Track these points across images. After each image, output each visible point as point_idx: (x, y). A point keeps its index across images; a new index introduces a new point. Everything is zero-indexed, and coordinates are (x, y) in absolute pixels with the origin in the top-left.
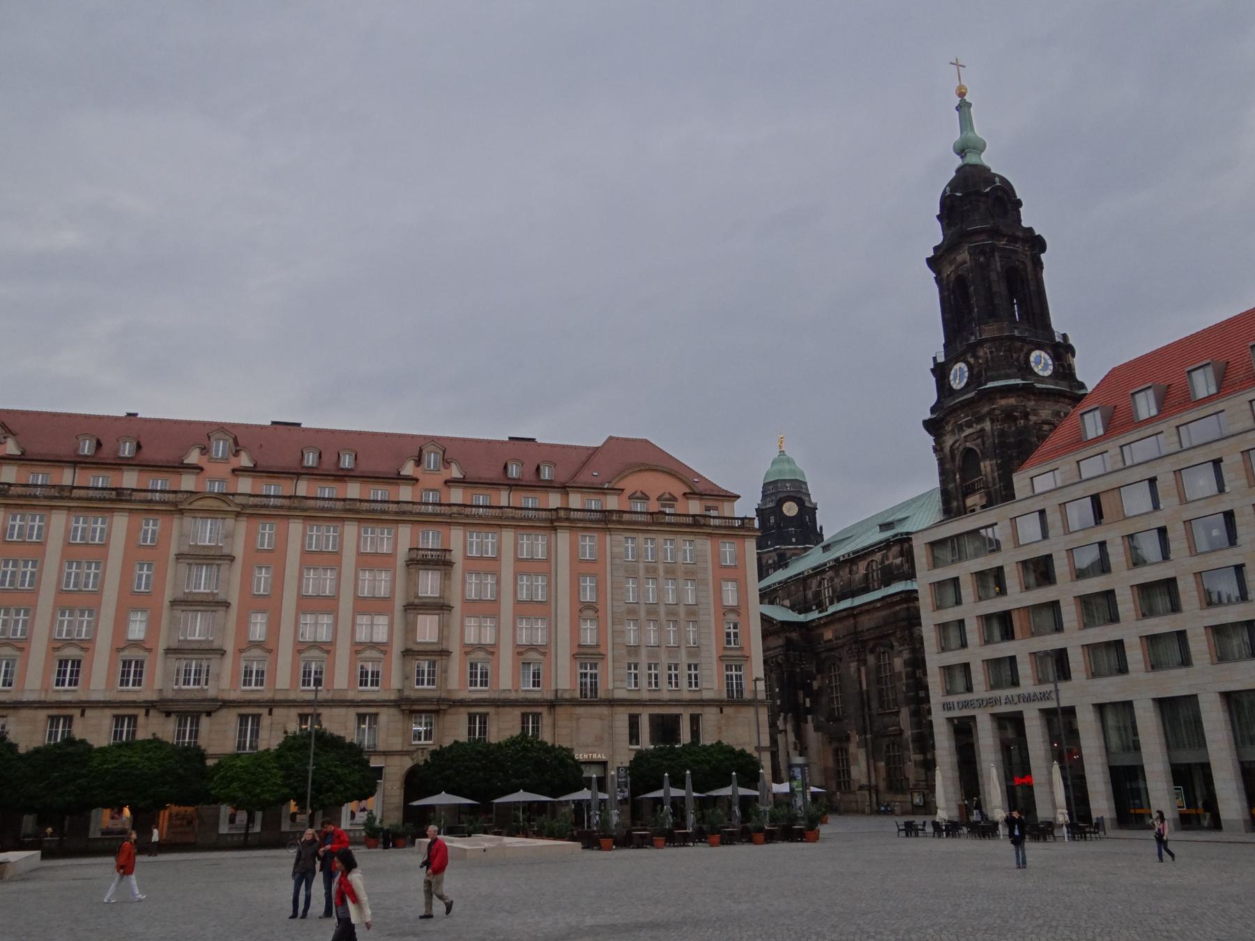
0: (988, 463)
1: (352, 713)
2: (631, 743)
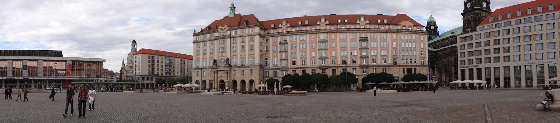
1: (352, 68)
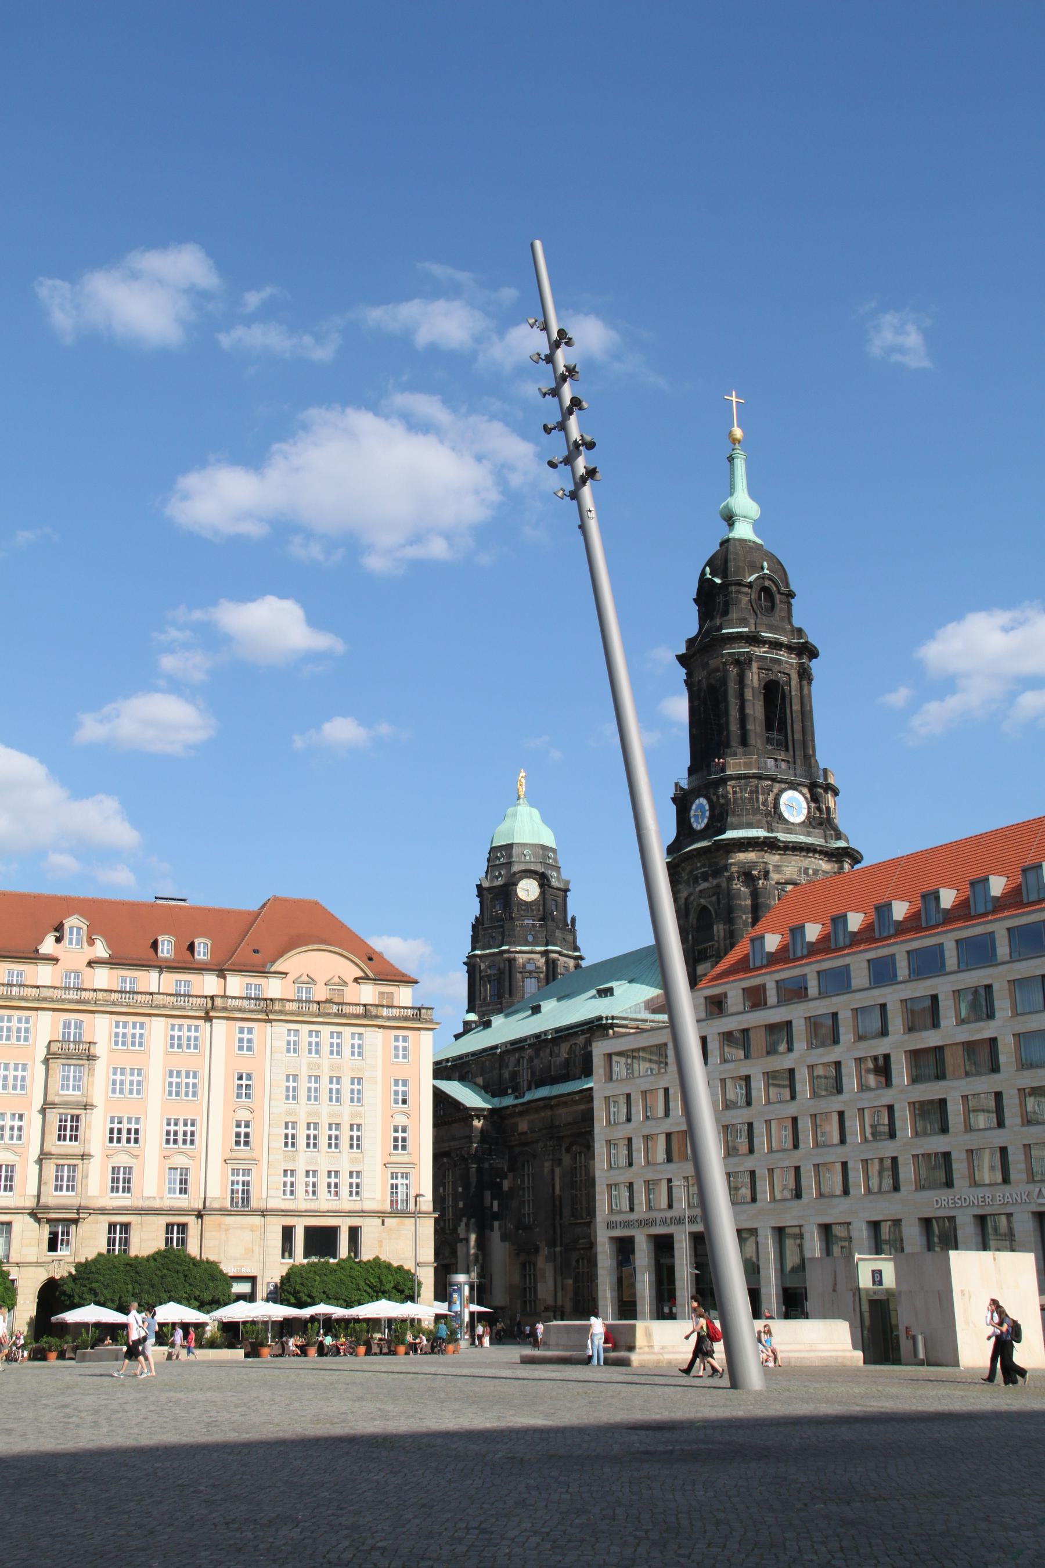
0: (721, 927)
2: (283, 1257)
